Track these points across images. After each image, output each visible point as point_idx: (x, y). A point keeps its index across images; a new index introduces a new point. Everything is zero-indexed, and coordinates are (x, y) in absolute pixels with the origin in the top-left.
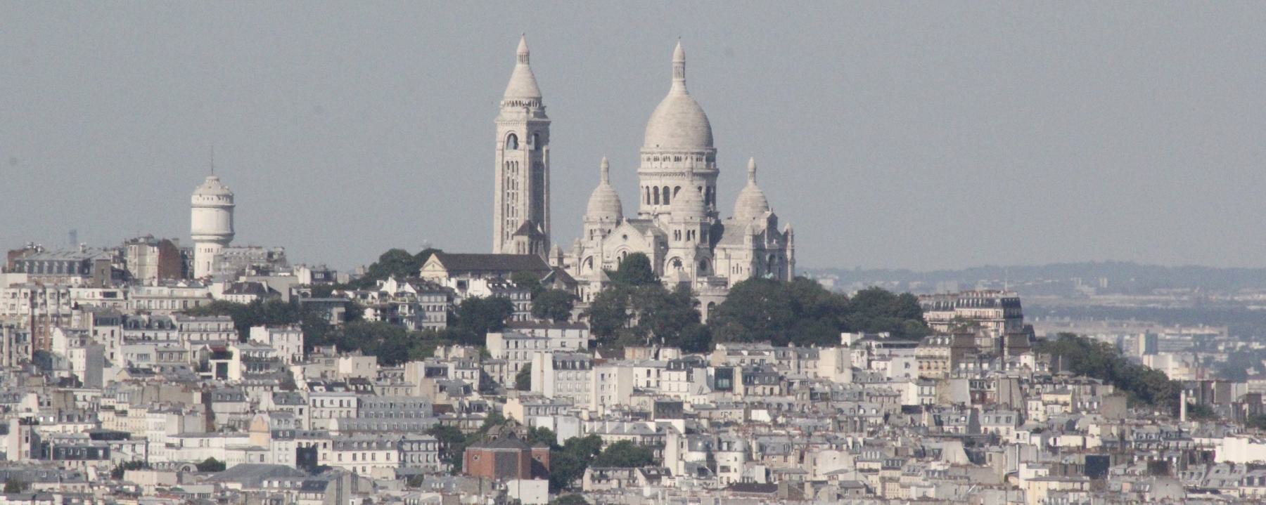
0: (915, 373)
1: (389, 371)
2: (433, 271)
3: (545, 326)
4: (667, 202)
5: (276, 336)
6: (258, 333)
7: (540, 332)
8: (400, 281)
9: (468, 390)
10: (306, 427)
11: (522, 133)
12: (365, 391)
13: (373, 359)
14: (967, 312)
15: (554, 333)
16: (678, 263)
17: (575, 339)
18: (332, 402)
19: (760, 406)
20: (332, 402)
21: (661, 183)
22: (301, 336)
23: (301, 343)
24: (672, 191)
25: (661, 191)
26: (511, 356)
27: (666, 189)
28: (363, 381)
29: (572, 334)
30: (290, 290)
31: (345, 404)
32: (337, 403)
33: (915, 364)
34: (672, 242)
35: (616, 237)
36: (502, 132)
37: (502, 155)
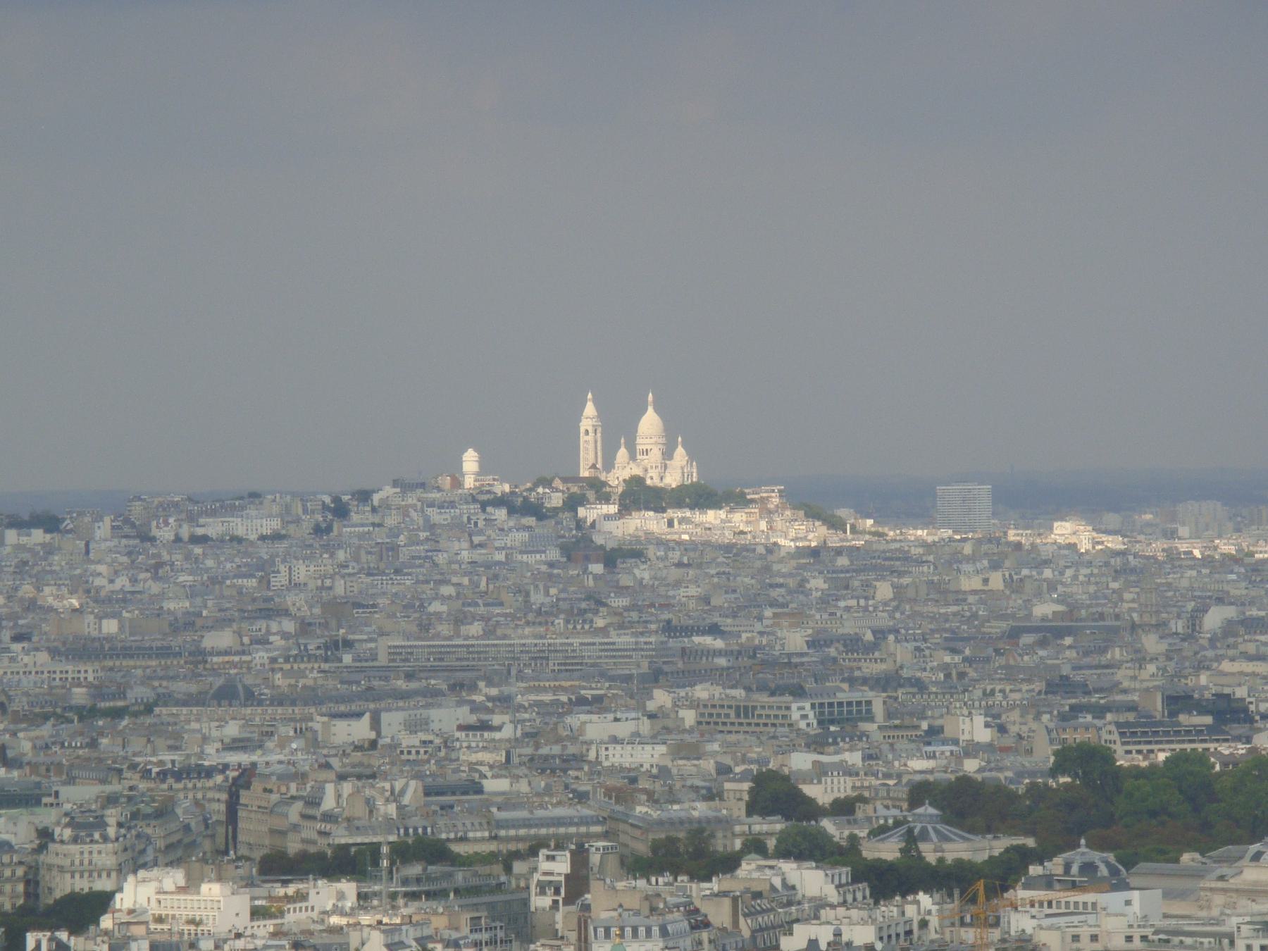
0: (744, 518)
1: (541, 523)
2: (558, 483)
3: (601, 504)
6: (489, 509)
7: (599, 506)
8: (544, 488)
9: (571, 530)
10: (509, 545)
11: (591, 430)
14: (765, 495)
15: (605, 507)
16: (652, 478)
17: (613, 509)
19: (685, 533)
21: (645, 448)
28: (531, 527)
29: (612, 506)
33: (744, 516)
34: (649, 470)
35: (628, 469)
36: (582, 430)
37: (583, 438)
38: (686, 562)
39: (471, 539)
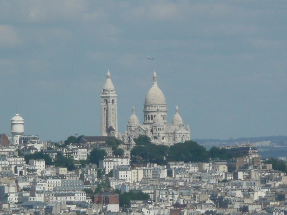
3: (117, 157)
4: (152, 119)
5: (37, 162)
7: (115, 160)
12: (64, 178)
13: (66, 169)
18: (54, 182)
20: (54, 182)
22: (45, 162)
23: (44, 164)
24: (153, 116)
25: (150, 116)
26: (107, 167)
27: (152, 116)
30: (41, 148)
31: (58, 183)
32: (55, 182)
38: (182, 203)
39: (17, 184)
